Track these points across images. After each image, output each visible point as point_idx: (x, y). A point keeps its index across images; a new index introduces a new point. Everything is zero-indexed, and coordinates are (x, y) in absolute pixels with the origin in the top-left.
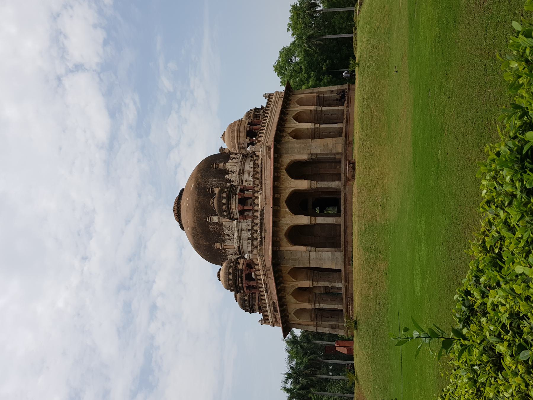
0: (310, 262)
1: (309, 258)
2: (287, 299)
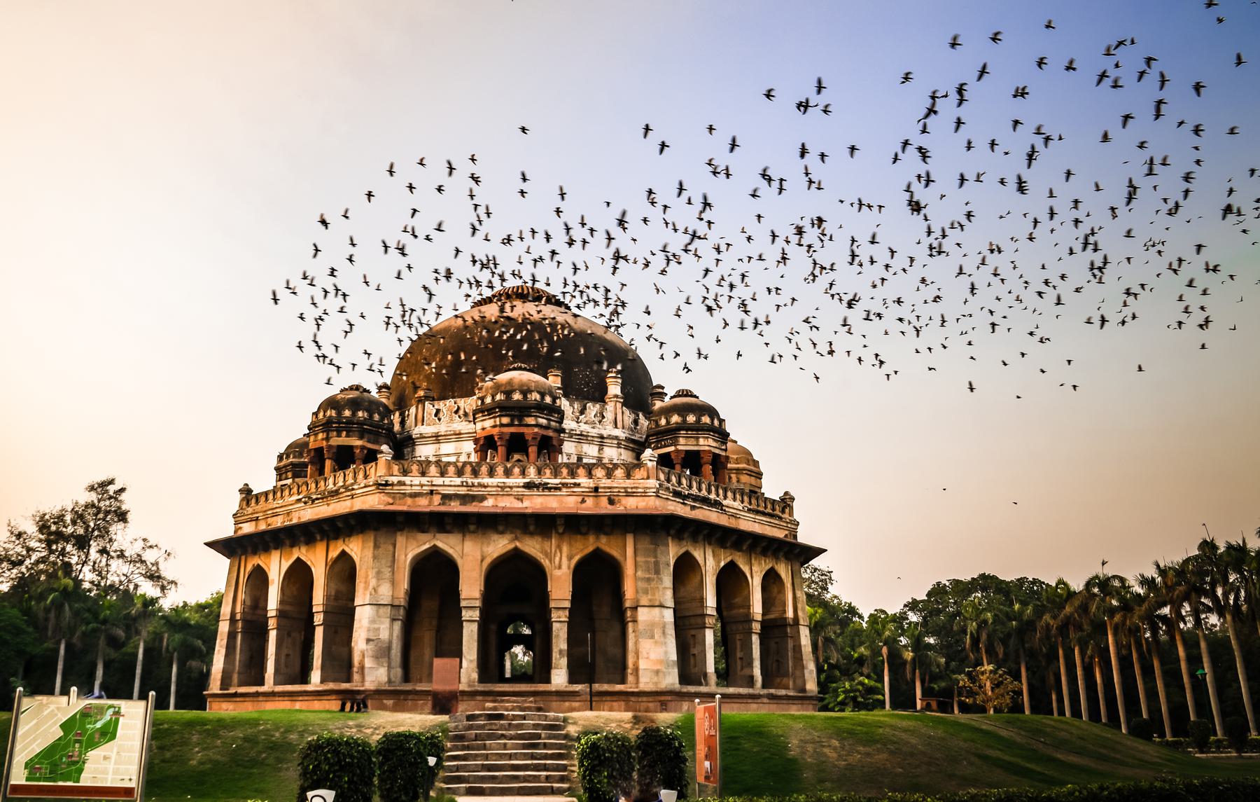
0: (657, 610)
1: (664, 607)
2: (495, 537)
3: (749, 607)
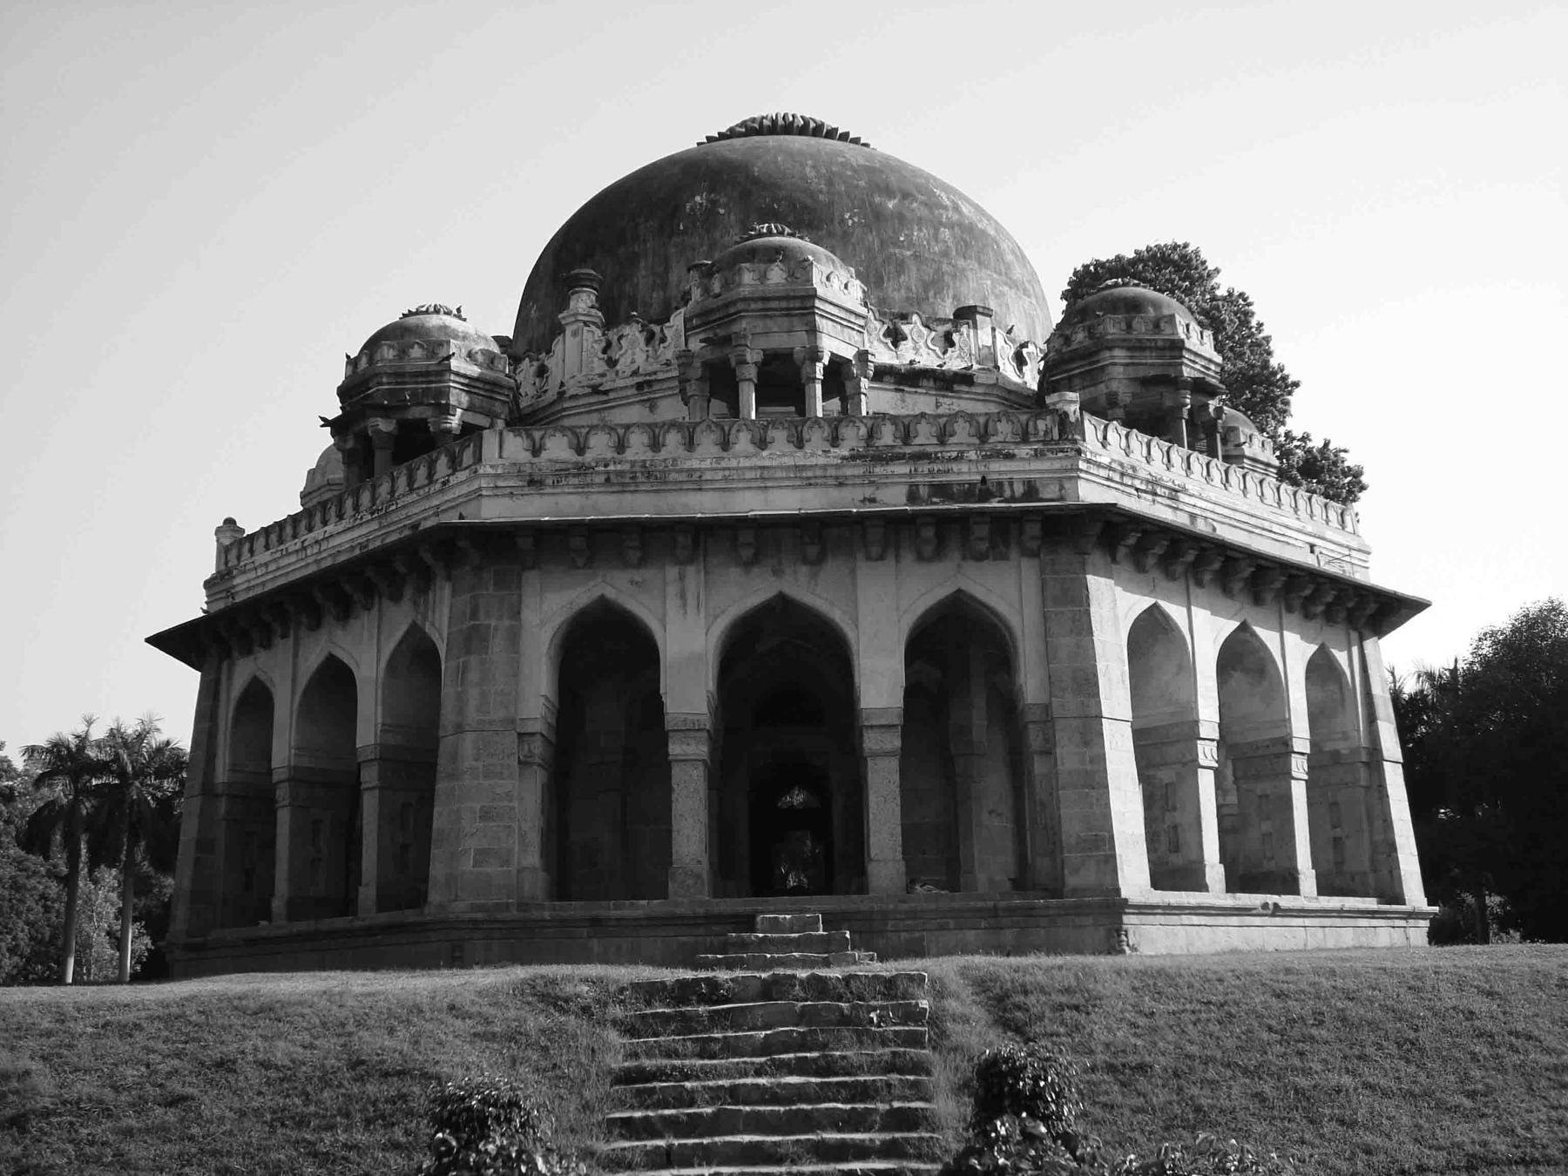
2: (734, 573)
3: (1286, 722)
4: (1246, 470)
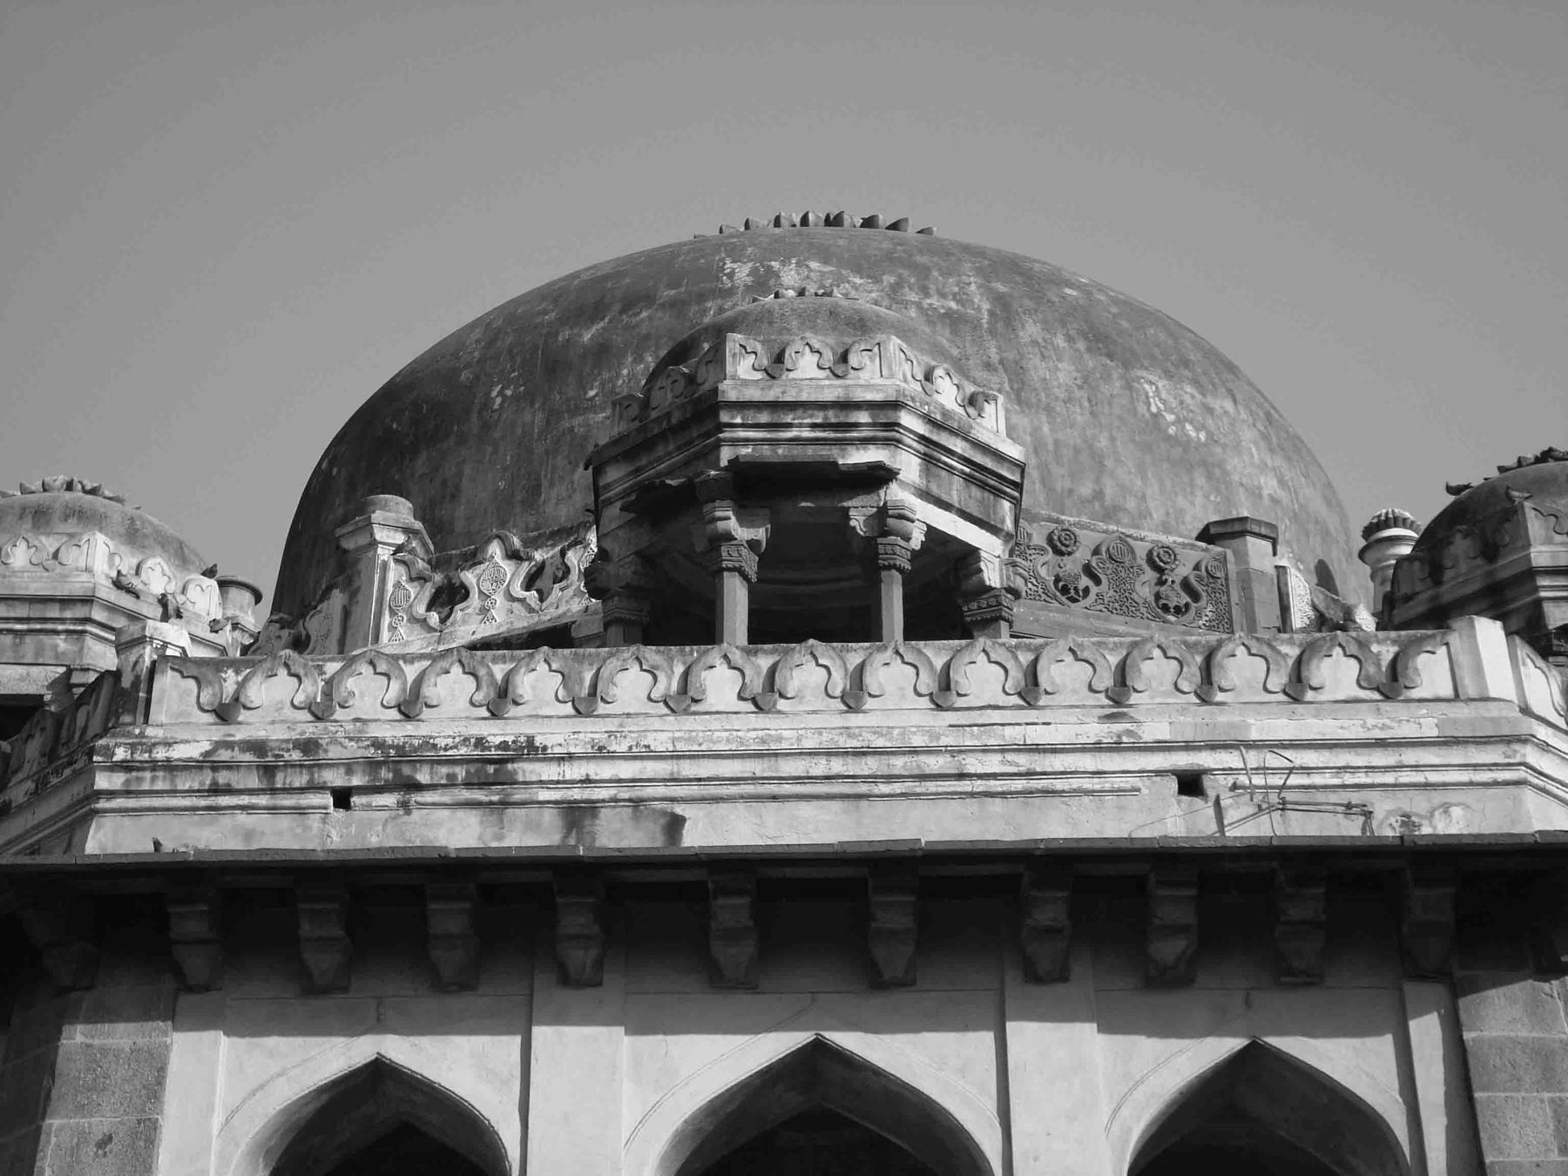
4: (411, 672)
